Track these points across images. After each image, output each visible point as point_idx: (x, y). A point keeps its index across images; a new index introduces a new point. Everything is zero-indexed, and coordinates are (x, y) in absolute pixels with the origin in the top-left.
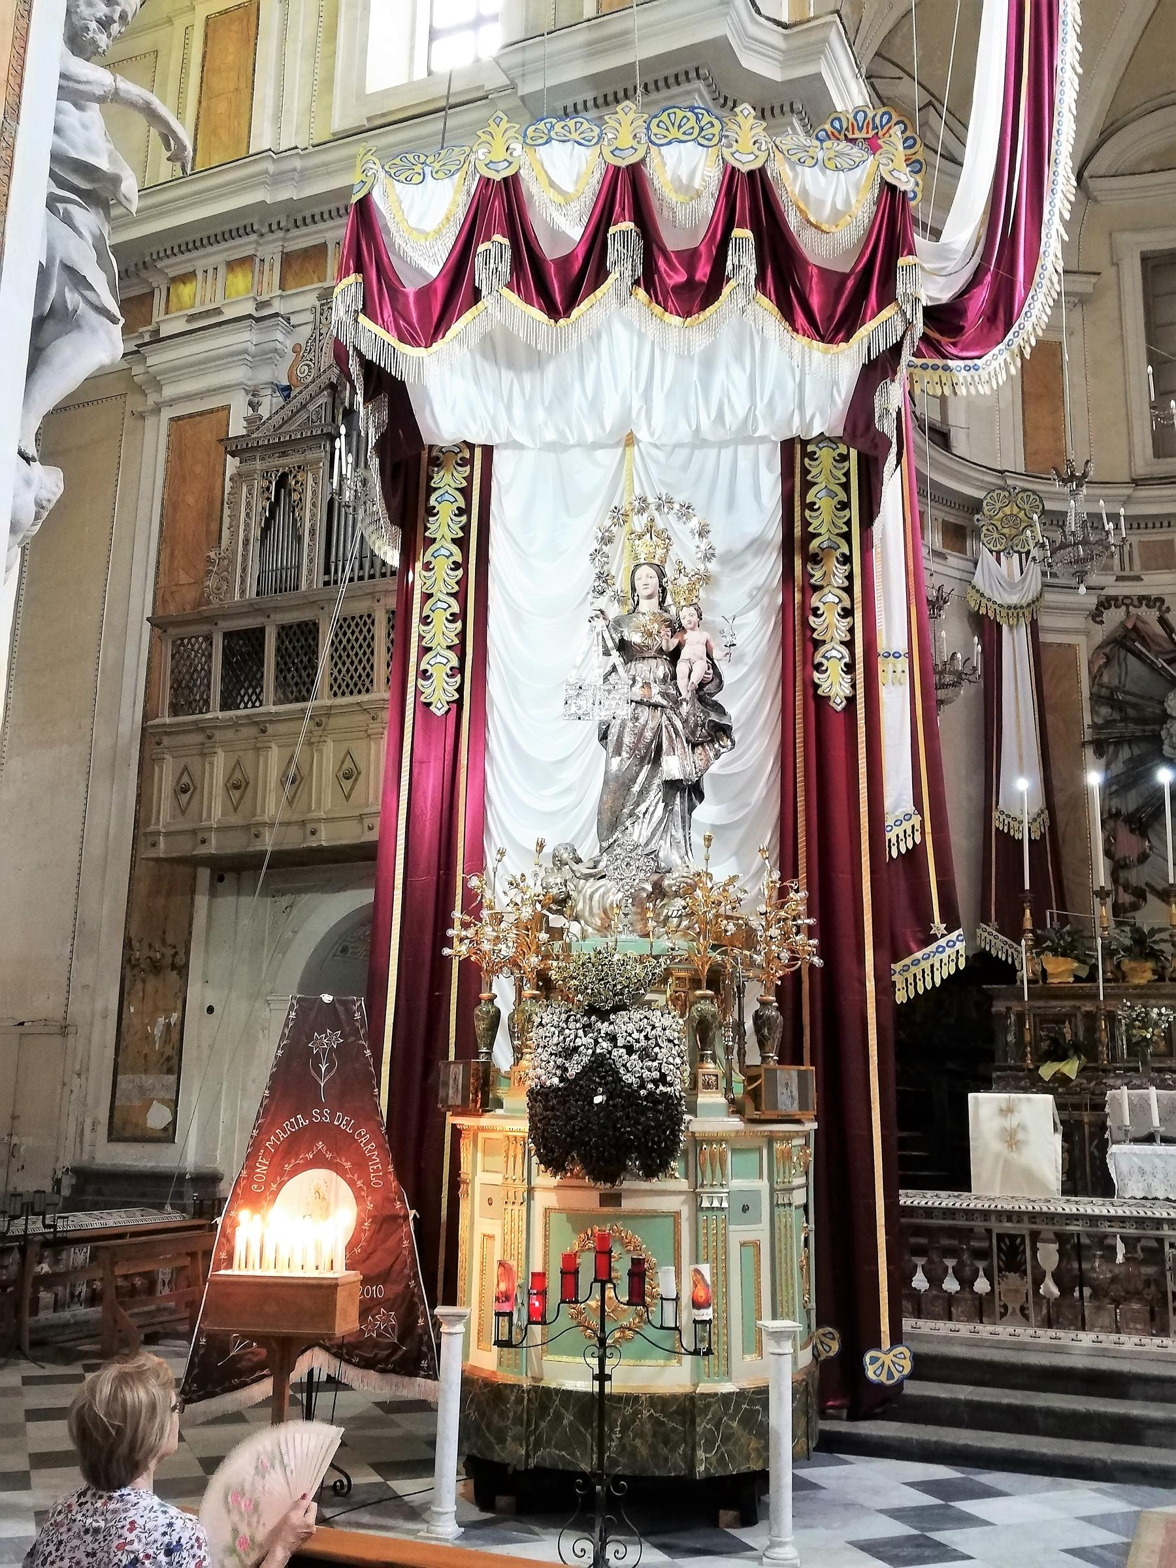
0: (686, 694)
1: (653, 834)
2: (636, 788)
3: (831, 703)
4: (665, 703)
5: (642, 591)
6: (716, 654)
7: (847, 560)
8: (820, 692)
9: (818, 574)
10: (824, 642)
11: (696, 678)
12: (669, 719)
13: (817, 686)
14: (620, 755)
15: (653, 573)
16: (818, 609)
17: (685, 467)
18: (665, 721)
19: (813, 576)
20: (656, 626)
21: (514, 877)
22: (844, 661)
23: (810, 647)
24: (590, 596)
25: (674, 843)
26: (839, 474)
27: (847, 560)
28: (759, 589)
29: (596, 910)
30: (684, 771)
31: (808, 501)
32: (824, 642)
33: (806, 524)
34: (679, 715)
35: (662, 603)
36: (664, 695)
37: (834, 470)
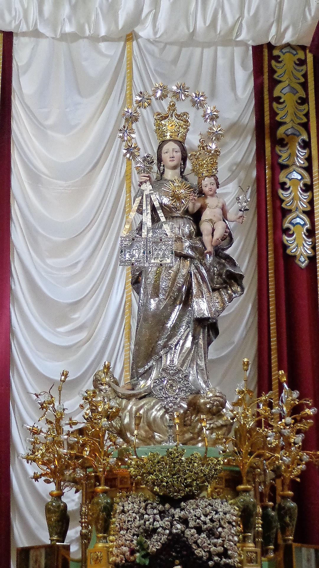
3: (297, 261)
7: (306, 145)
8: (288, 252)
10: (290, 211)
16: (285, 183)
17: (175, 61)
19: (280, 157)
22: (307, 227)
23: (279, 214)
26: (299, 75)
27: (306, 145)
28: (238, 165)
32: (290, 211)
33: (274, 114)
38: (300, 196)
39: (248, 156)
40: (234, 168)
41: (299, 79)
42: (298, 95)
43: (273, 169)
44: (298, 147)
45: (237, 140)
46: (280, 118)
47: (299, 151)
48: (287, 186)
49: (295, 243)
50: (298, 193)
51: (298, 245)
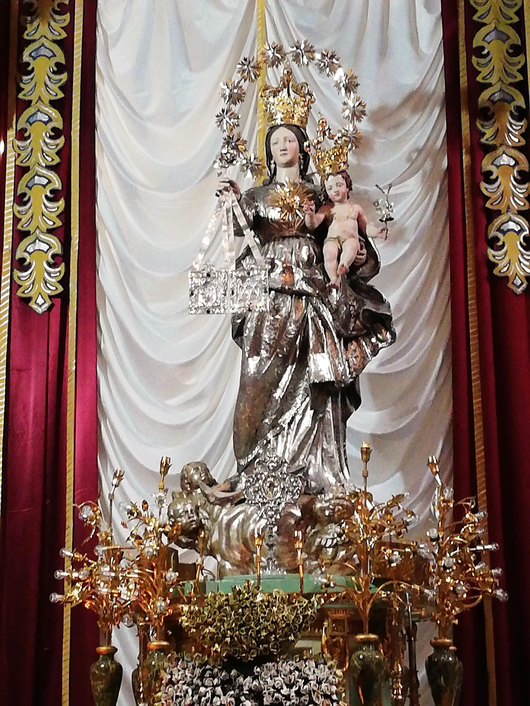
1: (301, 448)
2: (278, 394)
3: (510, 285)
4: (310, 290)
5: (279, 158)
6: (371, 230)
8: (496, 272)
9: (489, 132)
10: (498, 213)
11: (346, 259)
13: (495, 265)
14: (258, 354)
15: (291, 135)
16: (491, 173)
18: (311, 314)
20: (297, 199)
21: (134, 506)
22: (525, 233)
24: (216, 166)
25: (327, 459)
28: (420, 151)
29: (234, 542)
30: (336, 371)
31: (474, 46)
33: (473, 73)
34: (328, 304)
35: (303, 172)
36: (309, 280)
37: (504, 9)
38: (514, 190)
39: (437, 138)
40: (414, 156)
41: (511, 19)
42: (510, 42)
43: (472, 152)
44: (510, 118)
47: (511, 124)
48: (493, 177)
50: (511, 185)
51: (511, 262)
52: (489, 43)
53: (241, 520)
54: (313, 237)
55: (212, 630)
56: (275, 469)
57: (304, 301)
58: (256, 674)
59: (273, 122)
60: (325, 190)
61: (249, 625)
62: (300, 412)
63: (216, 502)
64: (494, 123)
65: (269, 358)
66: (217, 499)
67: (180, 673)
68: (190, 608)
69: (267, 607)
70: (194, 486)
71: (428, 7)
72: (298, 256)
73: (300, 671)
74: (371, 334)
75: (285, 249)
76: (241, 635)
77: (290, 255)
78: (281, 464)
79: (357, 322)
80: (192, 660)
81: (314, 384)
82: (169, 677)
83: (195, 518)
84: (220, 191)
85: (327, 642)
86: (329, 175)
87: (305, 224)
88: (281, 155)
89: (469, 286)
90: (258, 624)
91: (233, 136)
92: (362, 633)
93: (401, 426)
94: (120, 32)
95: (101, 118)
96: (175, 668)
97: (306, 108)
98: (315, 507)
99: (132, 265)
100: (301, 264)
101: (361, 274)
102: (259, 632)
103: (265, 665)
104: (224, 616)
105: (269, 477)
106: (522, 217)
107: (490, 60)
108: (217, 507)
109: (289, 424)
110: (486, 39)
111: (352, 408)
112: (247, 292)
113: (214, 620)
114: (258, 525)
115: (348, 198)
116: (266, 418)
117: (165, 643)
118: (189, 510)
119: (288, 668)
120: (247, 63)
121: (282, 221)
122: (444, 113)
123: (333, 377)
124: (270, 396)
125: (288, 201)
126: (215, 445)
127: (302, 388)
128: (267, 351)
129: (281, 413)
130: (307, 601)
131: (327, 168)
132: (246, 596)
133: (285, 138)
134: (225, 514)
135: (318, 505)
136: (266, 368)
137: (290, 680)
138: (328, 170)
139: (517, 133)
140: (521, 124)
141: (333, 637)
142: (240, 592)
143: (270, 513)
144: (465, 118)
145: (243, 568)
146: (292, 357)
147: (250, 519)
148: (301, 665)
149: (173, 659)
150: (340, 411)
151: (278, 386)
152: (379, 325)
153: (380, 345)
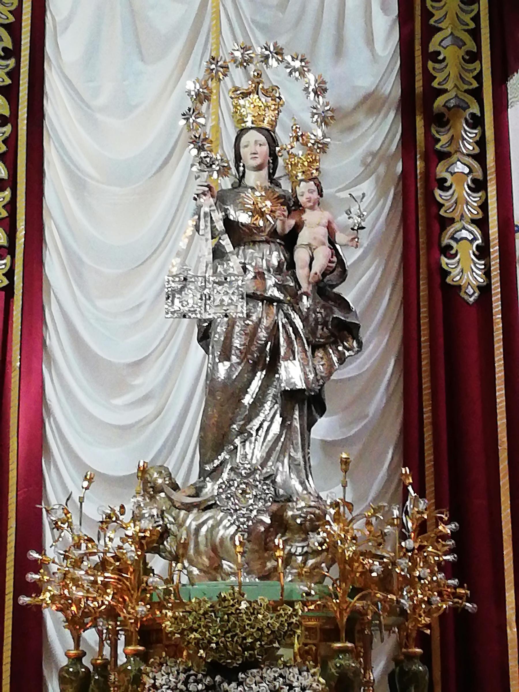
0: (305, 287)
1: (269, 455)
2: (248, 400)
3: (462, 294)
4: (281, 297)
5: (248, 160)
6: (340, 238)
8: (448, 280)
9: (444, 139)
10: (452, 221)
11: (318, 266)
12: (287, 316)
13: (447, 273)
14: (229, 359)
15: (262, 139)
16: (445, 180)
18: (282, 320)
20: (268, 203)
21: (112, 510)
22: (477, 242)
23: (436, 227)
24: (194, 169)
25: (293, 465)
26: (467, 18)
28: (374, 155)
29: (202, 548)
30: (306, 380)
31: (431, 49)
33: (429, 78)
34: (299, 312)
35: (271, 176)
36: (281, 287)
38: (468, 199)
39: (392, 141)
40: (369, 159)
41: (467, 25)
43: (426, 159)
44: (465, 125)
45: (374, 118)
46: (439, 84)
47: (465, 131)
48: (448, 184)
49: (460, 267)
51: (464, 272)
52: (445, 48)
53: (210, 526)
54: (283, 243)
55: (198, 636)
56: (248, 475)
57: (275, 307)
58: (241, 680)
59: (243, 125)
60: (296, 196)
61: (234, 631)
62: (269, 419)
63: (182, 507)
64: (449, 130)
65: (239, 364)
66: (182, 504)
67: (164, 678)
68: (174, 613)
69: (253, 614)
70: (158, 490)
71: (385, 8)
72: (268, 261)
73: (284, 678)
74: (338, 343)
75: (256, 254)
76: (226, 641)
77: (261, 260)
78: (253, 471)
79: (325, 329)
80: (175, 665)
81: (285, 391)
82: (153, 681)
83: (161, 523)
84: (198, 195)
85: (299, 649)
86: (301, 180)
87: (275, 230)
88: (252, 158)
89: (421, 294)
90: (243, 630)
91: (200, 136)
92: (338, 641)
93: (353, 432)
94: (69, 20)
95: (49, 107)
96: (160, 673)
97: (277, 112)
98: (286, 516)
99: (80, 259)
100: (271, 269)
101: (328, 281)
102: (244, 638)
103: (250, 672)
104: (209, 622)
105: (241, 484)
106: (475, 226)
107: (447, 66)
108: (183, 513)
109: (258, 430)
110: (442, 44)
111: (317, 416)
112: (224, 298)
113: (199, 626)
114: (228, 531)
115: (319, 204)
116: (234, 424)
117: (141, 648)
118: (155, 514)
119: (272, 675)
120: (215, 62)
121: (253, 225)
122: (399, 117)
123: (304, 385)
124: (240, 401)
125: (260, 205)
126: (164, 446)
127: (271, 395)
128: (238, 357)
129: (249, 419)
130: (291, 609)
131: (300, 174)
132: (232, 602)
133: (256, 142)
134: (194, 520)
135: (290, 513)
136: (237, 374)
137: (275, 686)
138: (300, 176)
139: (471, 141)
140: (476, 131)
141: (306, 645)
142: (225, 599)
143: (242, 520)
144: (420, 123)
145: (210, 573)
146: (262, 363)
147: (219, 525)
148: (285, 672)
149: (156, 665)
150: (306, 418)
151: (247, 392)
152: (346, 332)
153: (347, 354)
